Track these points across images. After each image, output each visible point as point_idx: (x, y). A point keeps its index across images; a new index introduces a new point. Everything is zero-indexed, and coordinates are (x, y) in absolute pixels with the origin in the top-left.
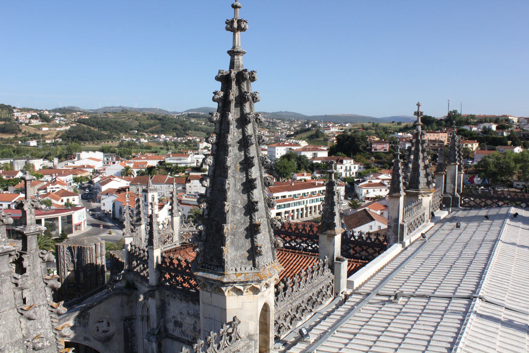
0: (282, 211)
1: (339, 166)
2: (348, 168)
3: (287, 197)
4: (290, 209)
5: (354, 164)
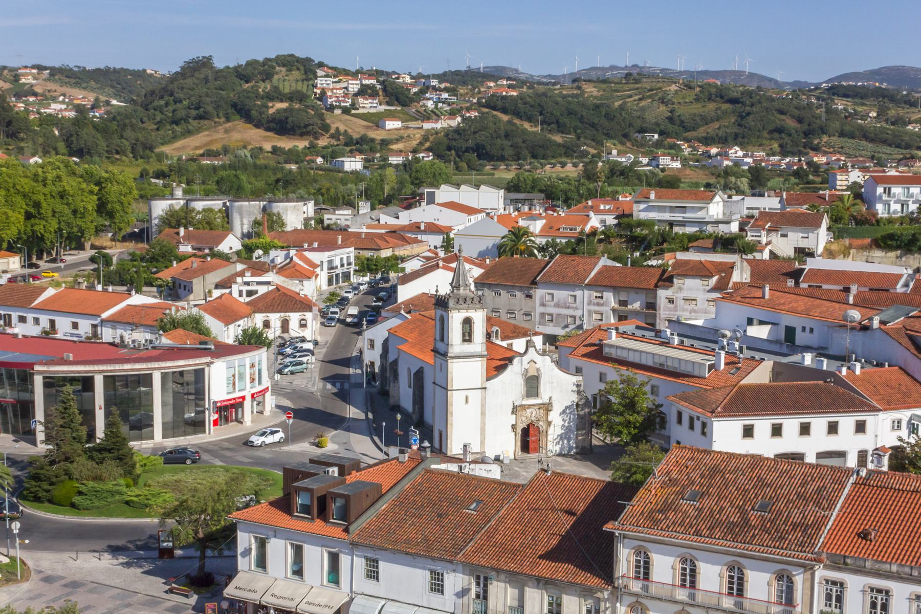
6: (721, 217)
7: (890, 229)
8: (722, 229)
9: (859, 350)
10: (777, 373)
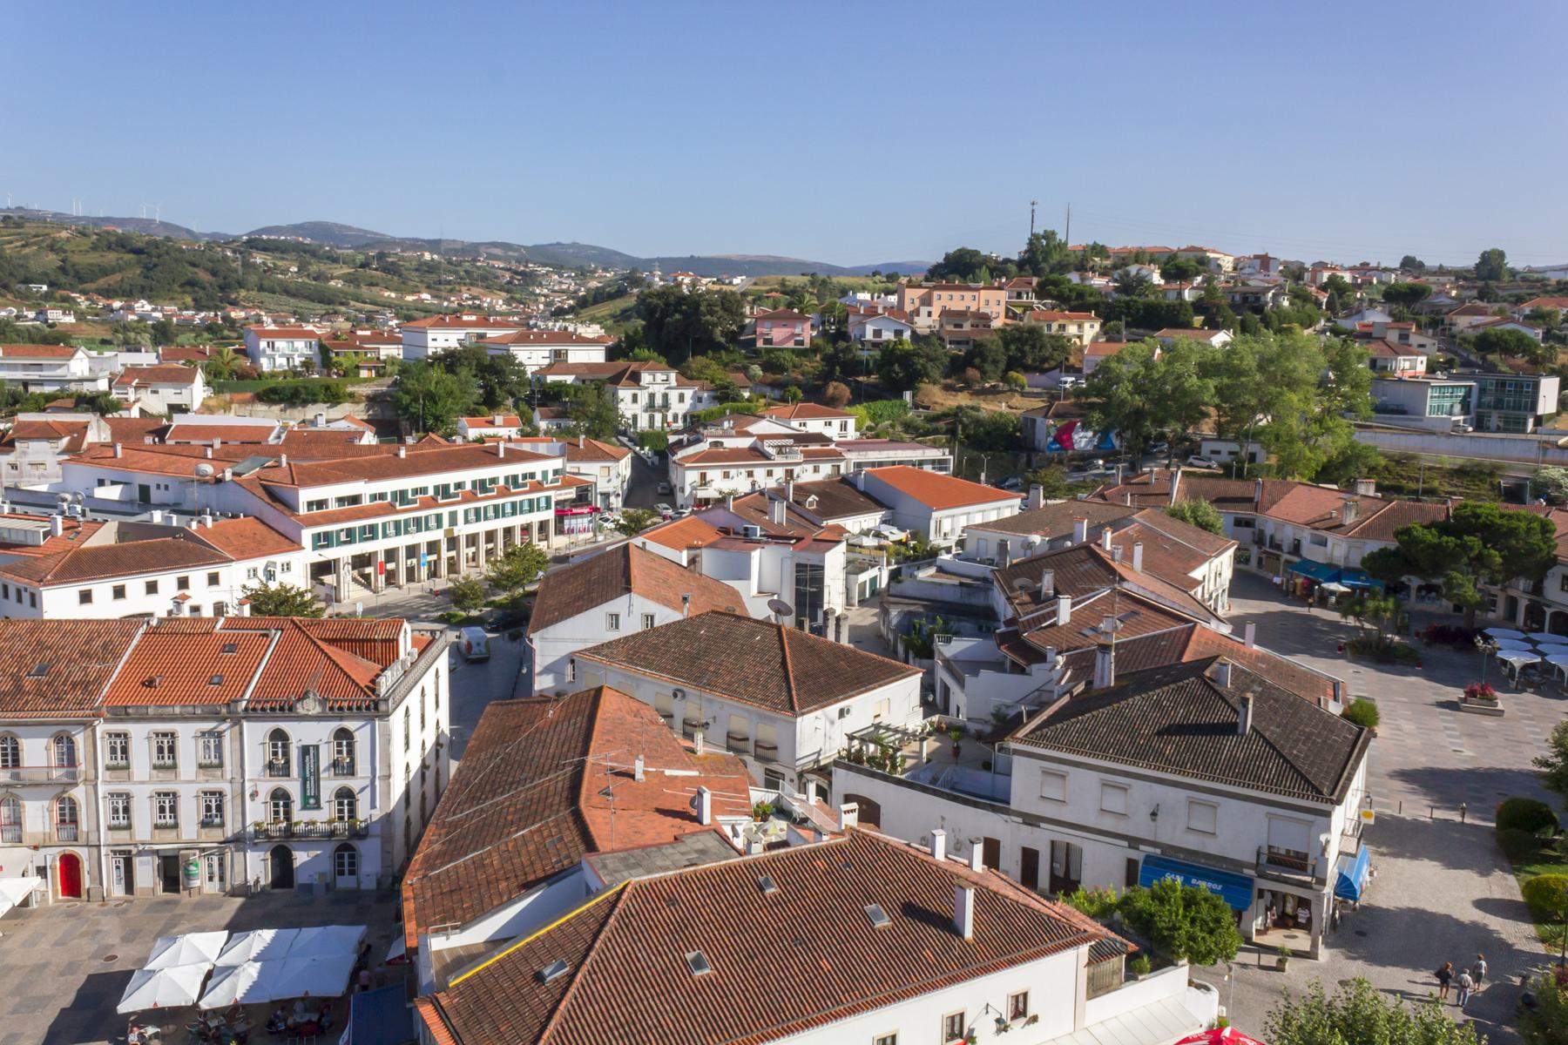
0: (343, 553)
1: (625, 394)
2: (659, 401)
3: (366, 502)
4: (379, 546)
5: (679, 386)
6: (87, 374)
7: (272, 383)
8: (87, 388)
9: (214, 504)
10: (123, 532)
